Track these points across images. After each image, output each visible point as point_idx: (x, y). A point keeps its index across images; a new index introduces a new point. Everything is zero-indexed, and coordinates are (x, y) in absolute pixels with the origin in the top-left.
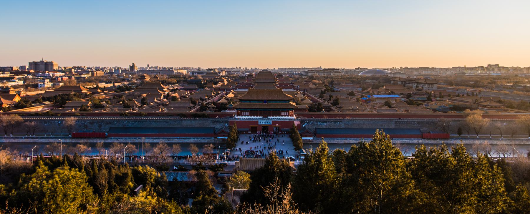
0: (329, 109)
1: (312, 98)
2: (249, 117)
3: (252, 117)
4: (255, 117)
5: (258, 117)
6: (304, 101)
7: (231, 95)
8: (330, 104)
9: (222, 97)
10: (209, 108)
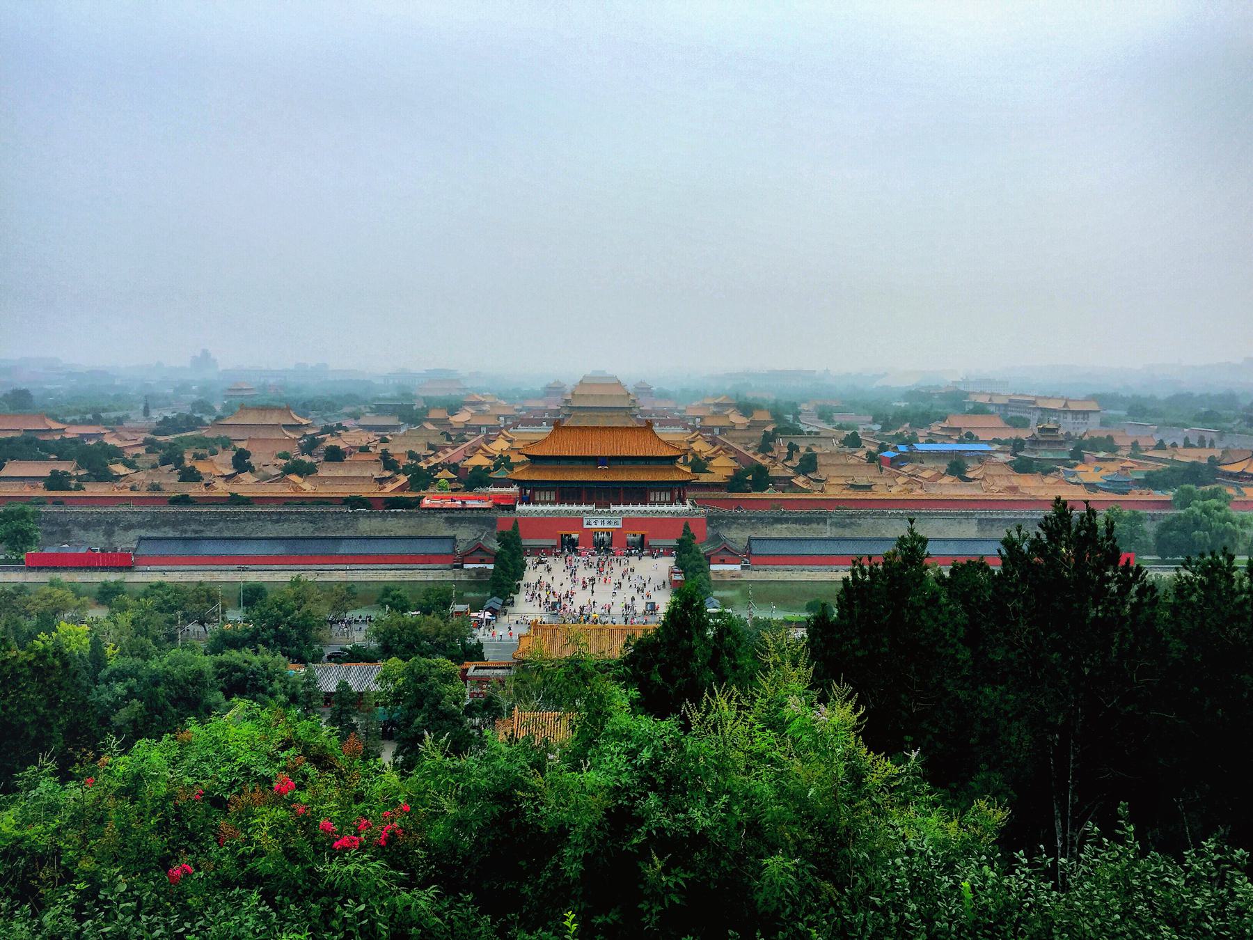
0: (788, 484)
1: (737, 452)
2: (557, 507)
3: (566, 507)
5: (583, 507)
6: (714, 462)
7: (499, 446)
8: (791, 471)
9: (475, 450)
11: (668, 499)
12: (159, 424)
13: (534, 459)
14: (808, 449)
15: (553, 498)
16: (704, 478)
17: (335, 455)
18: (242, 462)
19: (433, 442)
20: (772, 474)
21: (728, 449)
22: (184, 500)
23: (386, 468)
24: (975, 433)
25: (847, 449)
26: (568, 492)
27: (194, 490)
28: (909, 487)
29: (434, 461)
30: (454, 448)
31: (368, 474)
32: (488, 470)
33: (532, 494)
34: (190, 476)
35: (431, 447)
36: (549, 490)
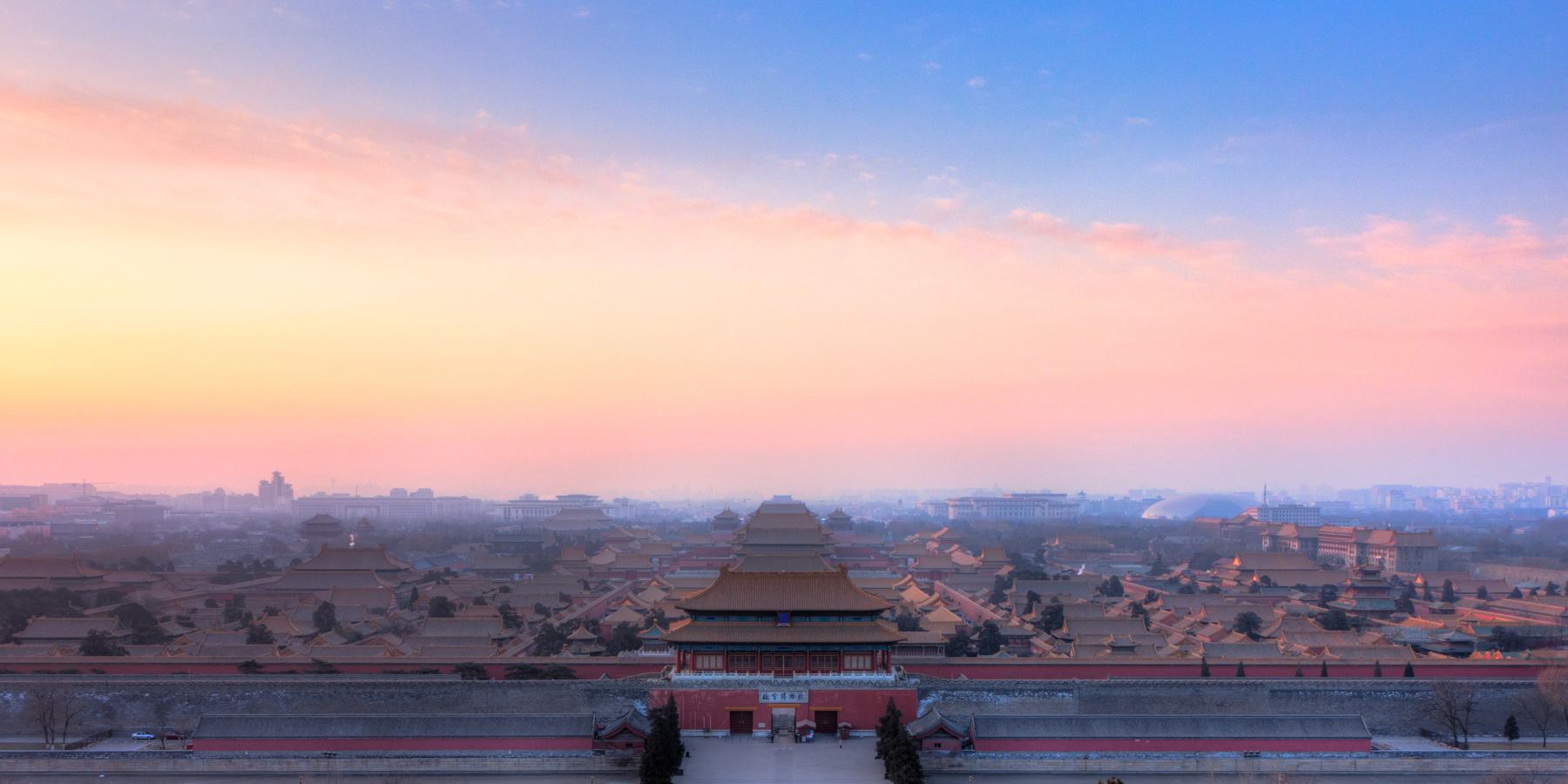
3: (735, 676)
4: (747, 677)
5: (758, 676)
6: (931, 617)
7: (653, 596)
10: (570, 642)
11: (868, 666)
12: (220, 568)
13: (695, 614)
14: (1054, 599)
15: (720, 665)
16: (914, 638)
17: (442, 609)
18: (325, 619)
19: (565, 592)
20: (1002, 633)
21: (947, 601)
22: (250, 667)
23: (507, 626)
24: (1274, 578)
25: (1106, 599)
26: (737, 655)
27: (263, 655)
28: (1184, 648)
29: (568, 616)
30: (592, 599)
31: (484, 634)
32: (637, 629)
33: (694, 660)
34: (260, 637)
35: (564, 598)
36: (716, 654)
